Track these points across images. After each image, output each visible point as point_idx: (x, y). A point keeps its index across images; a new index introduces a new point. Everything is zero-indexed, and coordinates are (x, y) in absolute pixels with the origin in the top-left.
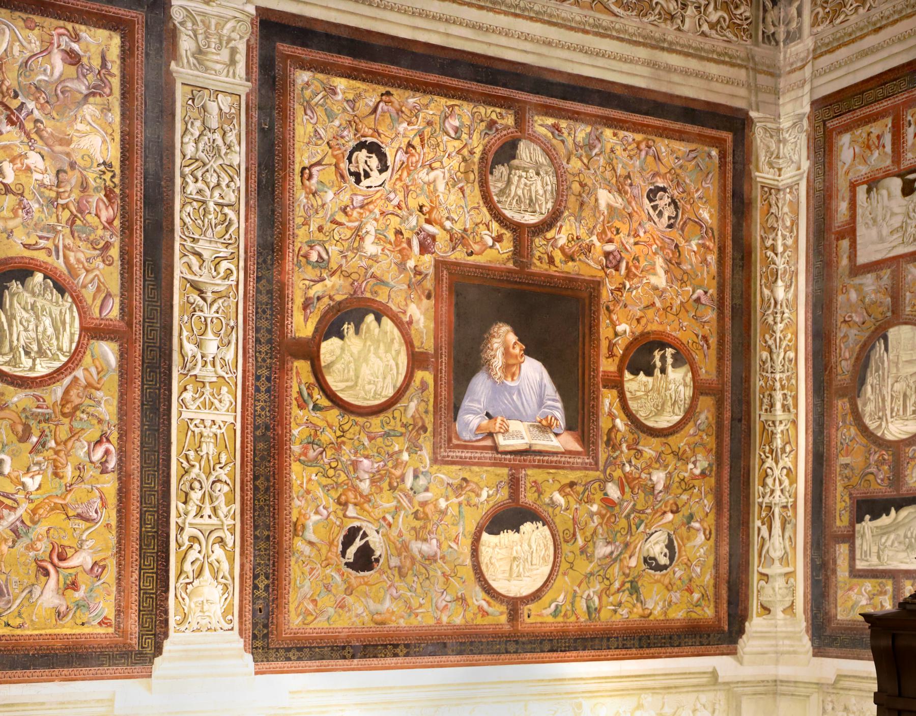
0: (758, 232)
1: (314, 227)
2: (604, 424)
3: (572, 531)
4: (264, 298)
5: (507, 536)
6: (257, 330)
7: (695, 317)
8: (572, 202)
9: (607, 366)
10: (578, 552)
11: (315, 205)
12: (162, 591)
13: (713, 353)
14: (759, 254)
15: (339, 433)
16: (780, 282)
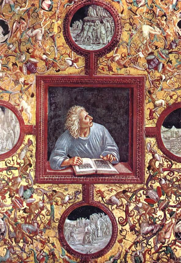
3: (125, 218)
9: (149, 124)
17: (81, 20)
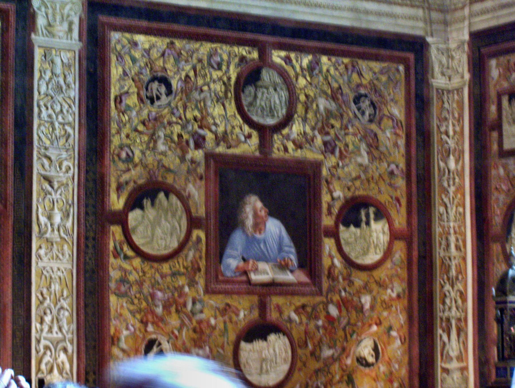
0: (435, 122)
1: (123, 136)
2: (326, 262)
4: (91, 185)
5: (259, 344)
6: (87, 206)
7: (390, 185)
8: (300, 109)
9: (327, 221)
10: (309, 355)
11: (124, 120)
13: (403, 210)
14: (436, 138)
15: (141, 274)
16: (452, 157)
17: (253, 85)
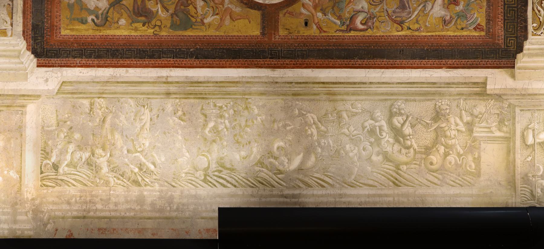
12: (522, 6)
